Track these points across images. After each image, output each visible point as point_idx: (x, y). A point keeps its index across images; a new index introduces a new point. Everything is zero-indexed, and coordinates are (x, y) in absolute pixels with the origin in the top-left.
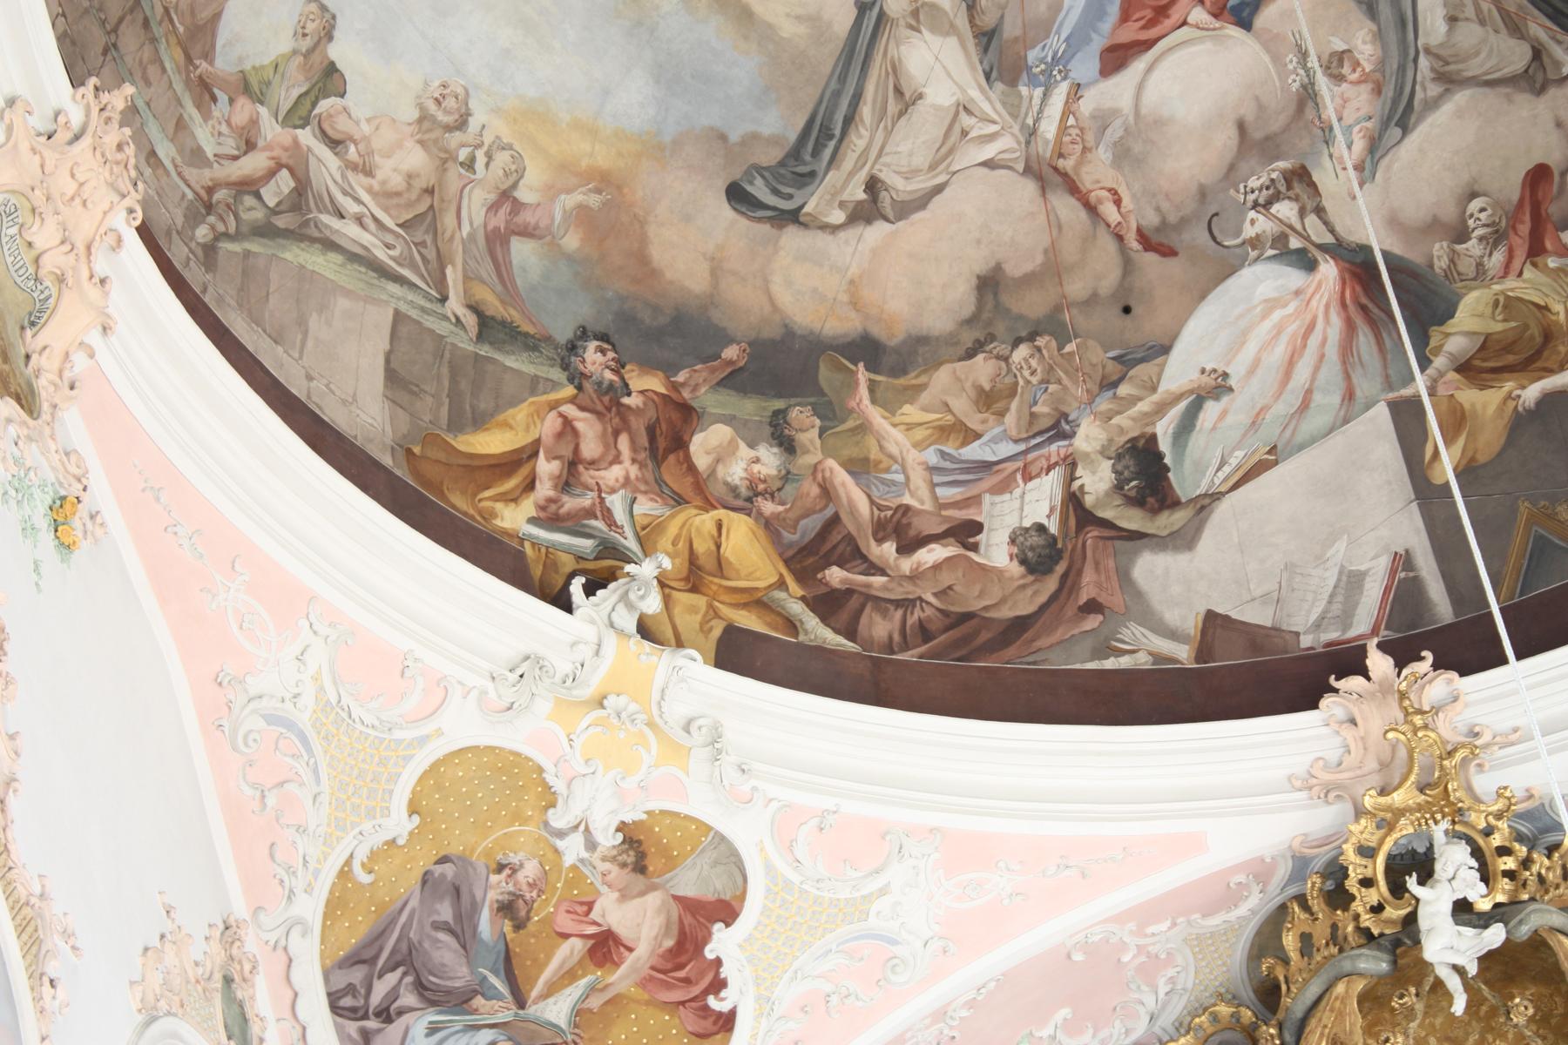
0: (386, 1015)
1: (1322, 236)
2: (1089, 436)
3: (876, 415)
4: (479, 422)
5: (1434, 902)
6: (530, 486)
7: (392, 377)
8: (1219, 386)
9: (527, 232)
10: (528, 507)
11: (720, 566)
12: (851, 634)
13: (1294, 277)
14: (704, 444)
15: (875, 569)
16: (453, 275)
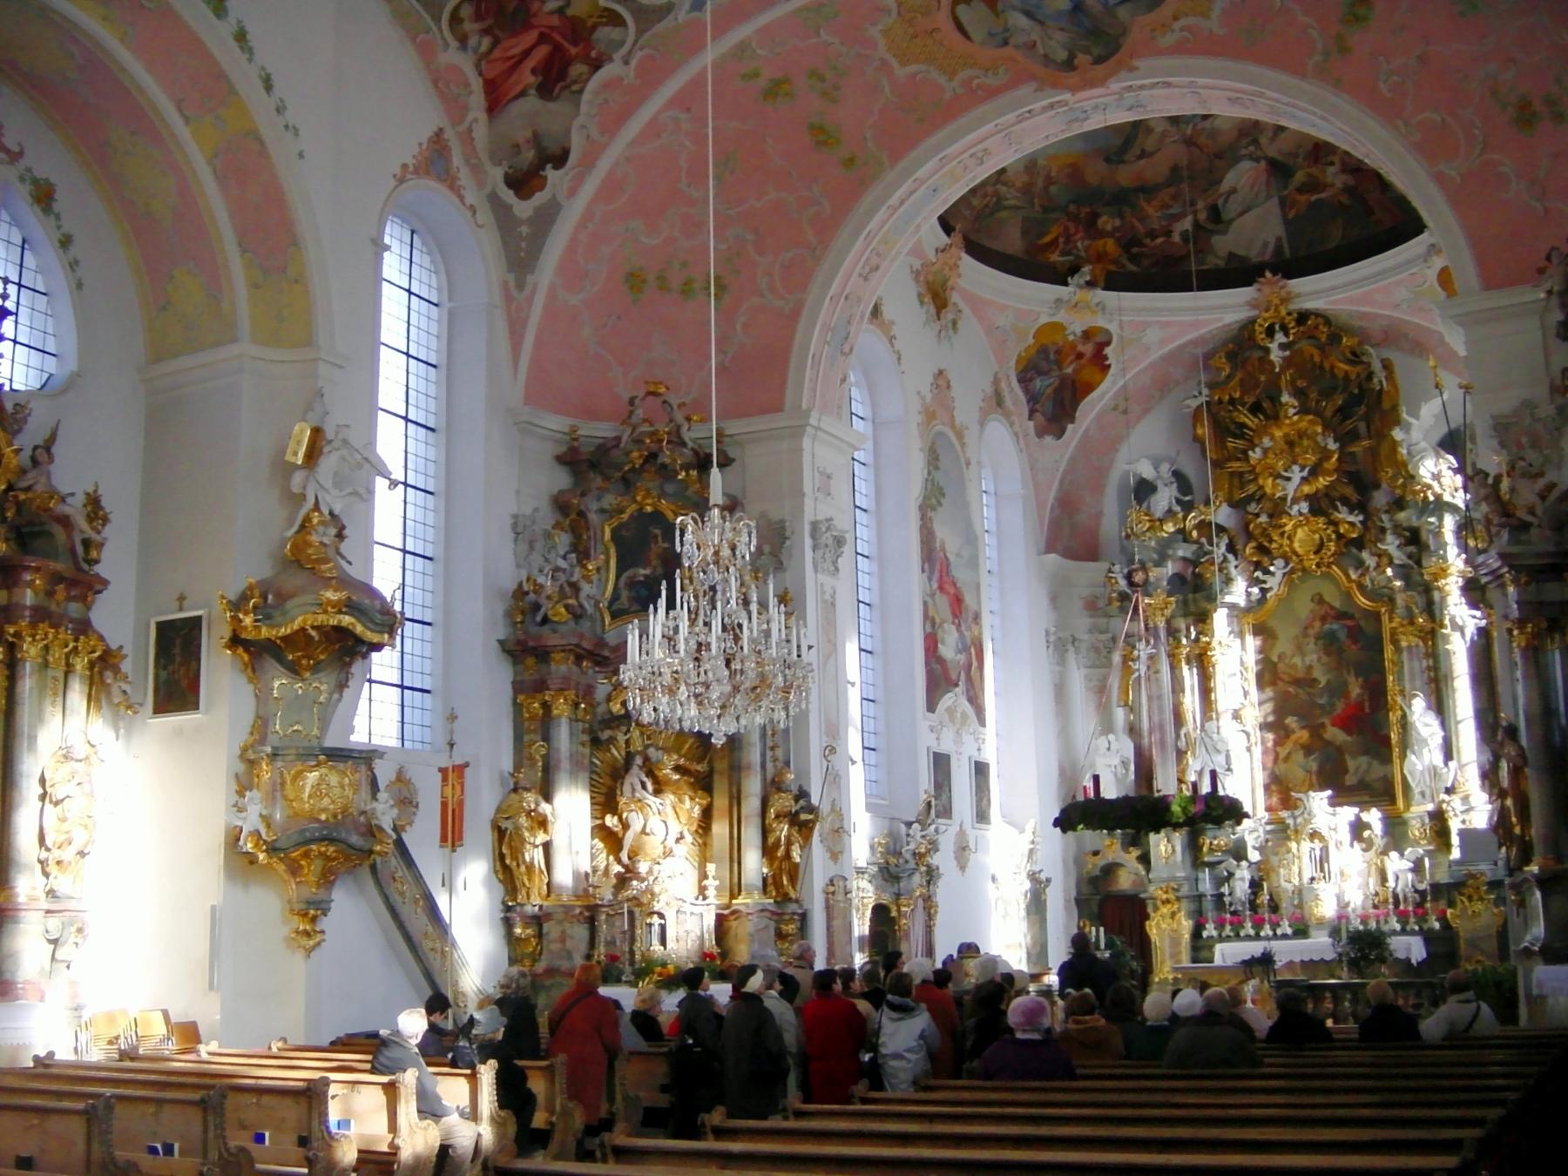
0: (1031, 380)
1: (1259, 153)
2: (1200, 205)
3: (1144, 204)
4: (1042, 235)
5: (1274, 346)
6: (1058, 246)
7: (1025, 233)
8: (1234, 191)
9: (1053, 184)
10: (1057, 252)
11: (1106, 253)
12: (1138, 265)
13: (1255, 164)
14: (1101, 221)
15: (1146, 246)
16: (1036, 201)
